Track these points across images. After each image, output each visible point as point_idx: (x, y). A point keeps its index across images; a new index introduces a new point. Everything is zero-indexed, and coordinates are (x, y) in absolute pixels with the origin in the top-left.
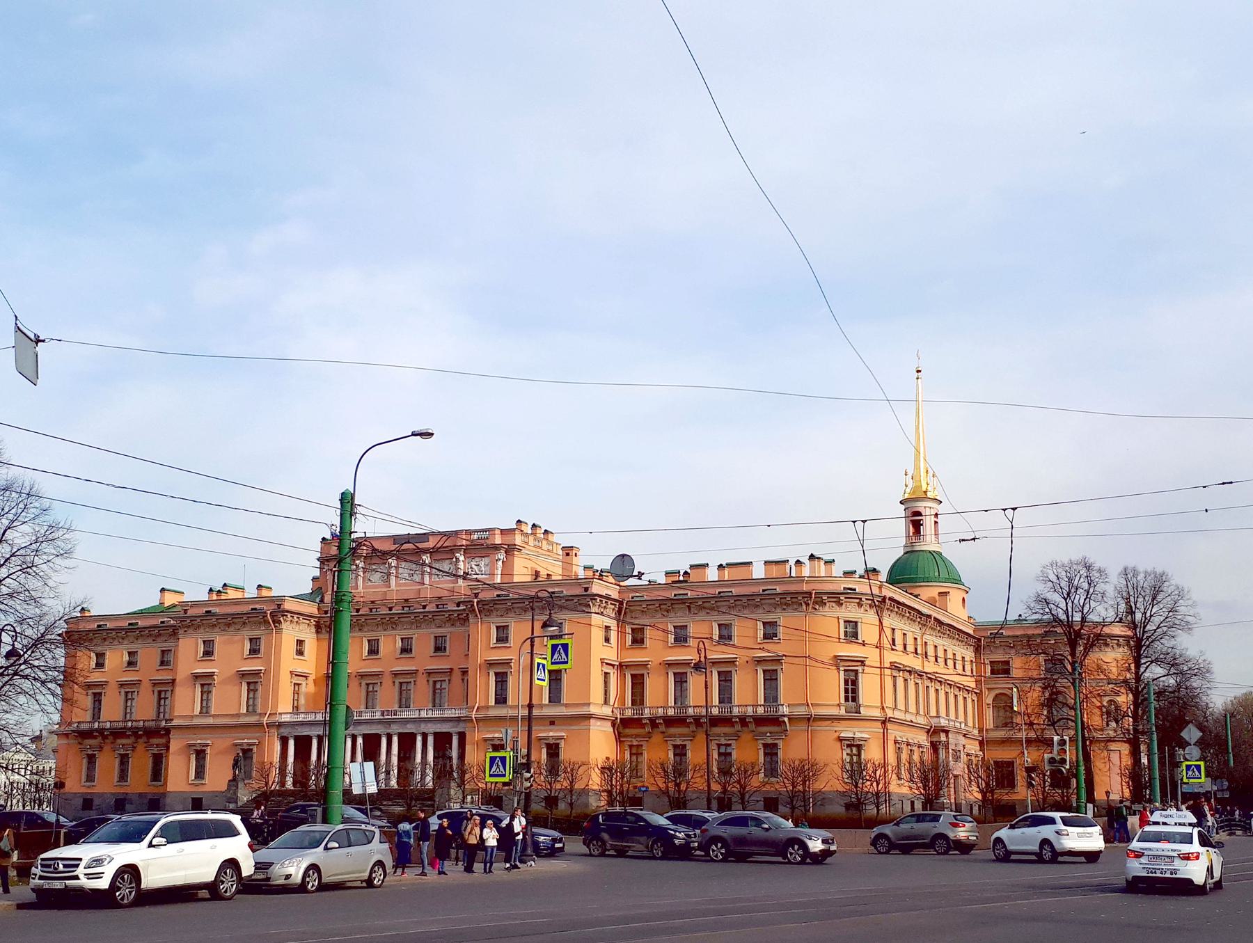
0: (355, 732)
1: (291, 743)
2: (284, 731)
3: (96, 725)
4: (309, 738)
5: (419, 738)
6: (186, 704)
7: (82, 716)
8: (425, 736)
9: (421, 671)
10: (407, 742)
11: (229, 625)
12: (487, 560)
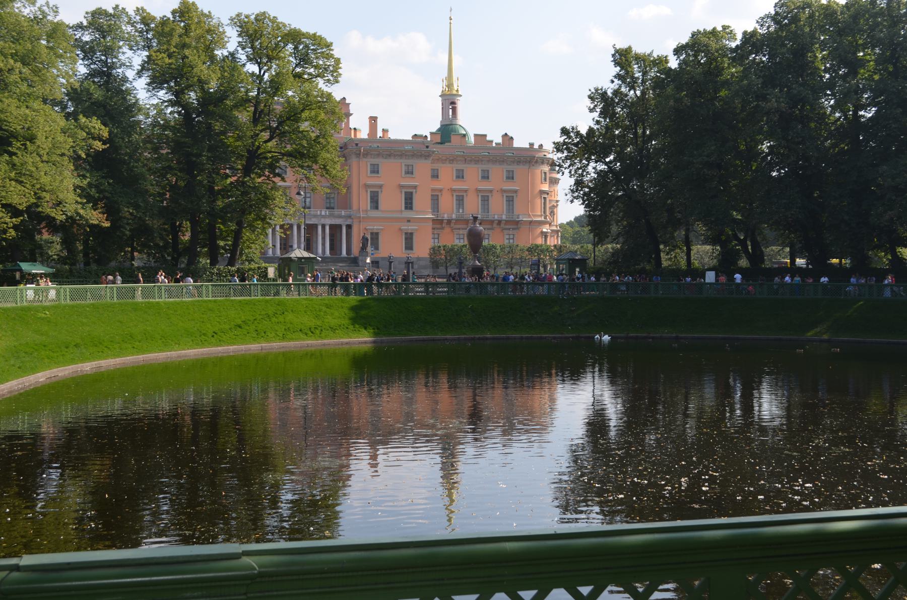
5: (320, 228)
8: (323, 226)
10: (311, 229)
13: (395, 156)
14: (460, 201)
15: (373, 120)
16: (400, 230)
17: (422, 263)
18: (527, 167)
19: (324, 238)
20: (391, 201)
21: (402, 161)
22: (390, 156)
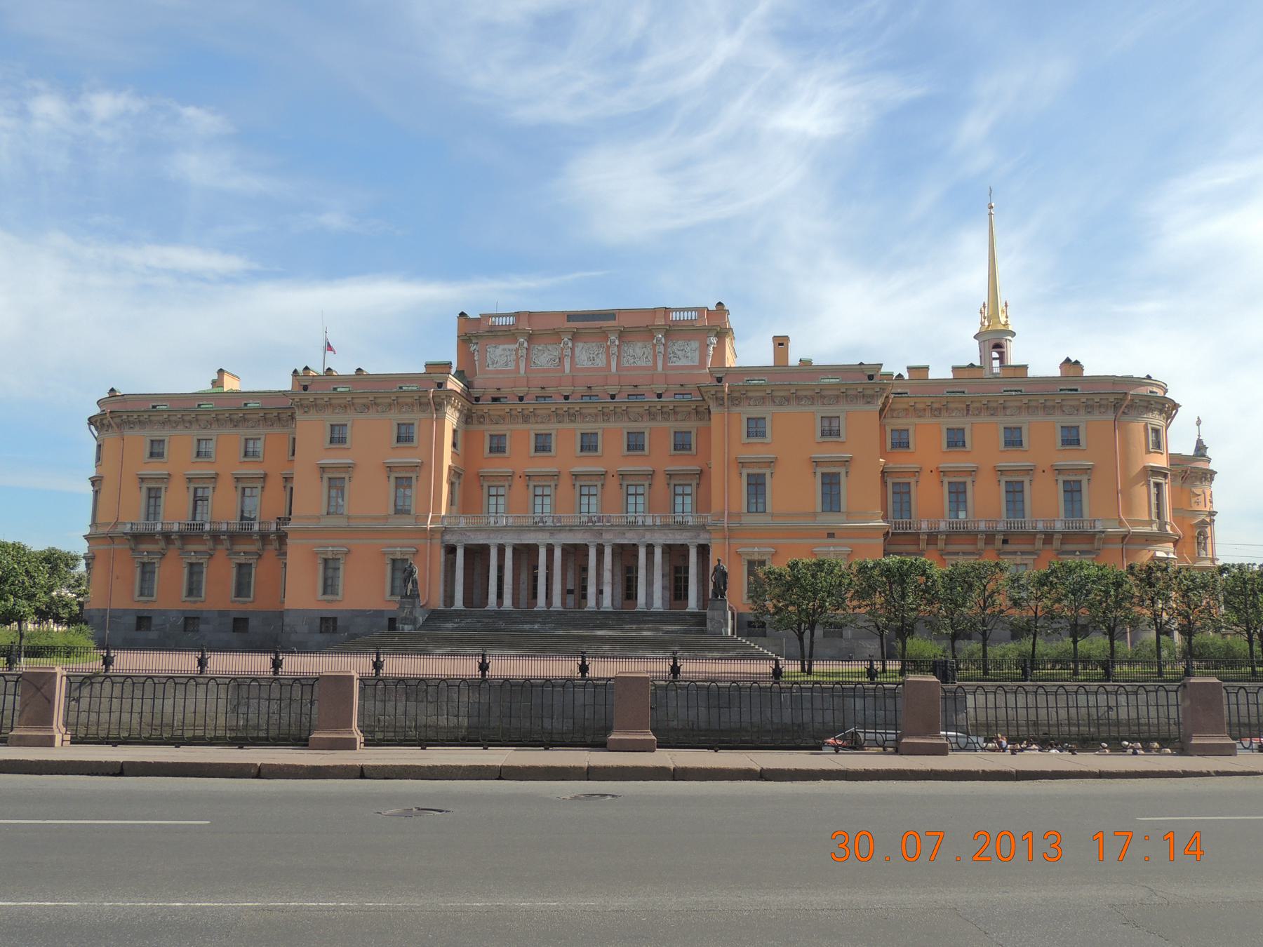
0: (550, 541)
1: (460, 553)
2: (451, 539)
3: (159, 527)
4: (485, 549)
6: (310, 499)
7: (133, 516)
8: (650, 548)
11: (367, 407)
12: (695, 345)
13: (799, 399)
14: (958, 494)
15: (781, 343)
18: (1110, 416)
20: (794, 492)
21: (813, 408)
22: (788, 399)
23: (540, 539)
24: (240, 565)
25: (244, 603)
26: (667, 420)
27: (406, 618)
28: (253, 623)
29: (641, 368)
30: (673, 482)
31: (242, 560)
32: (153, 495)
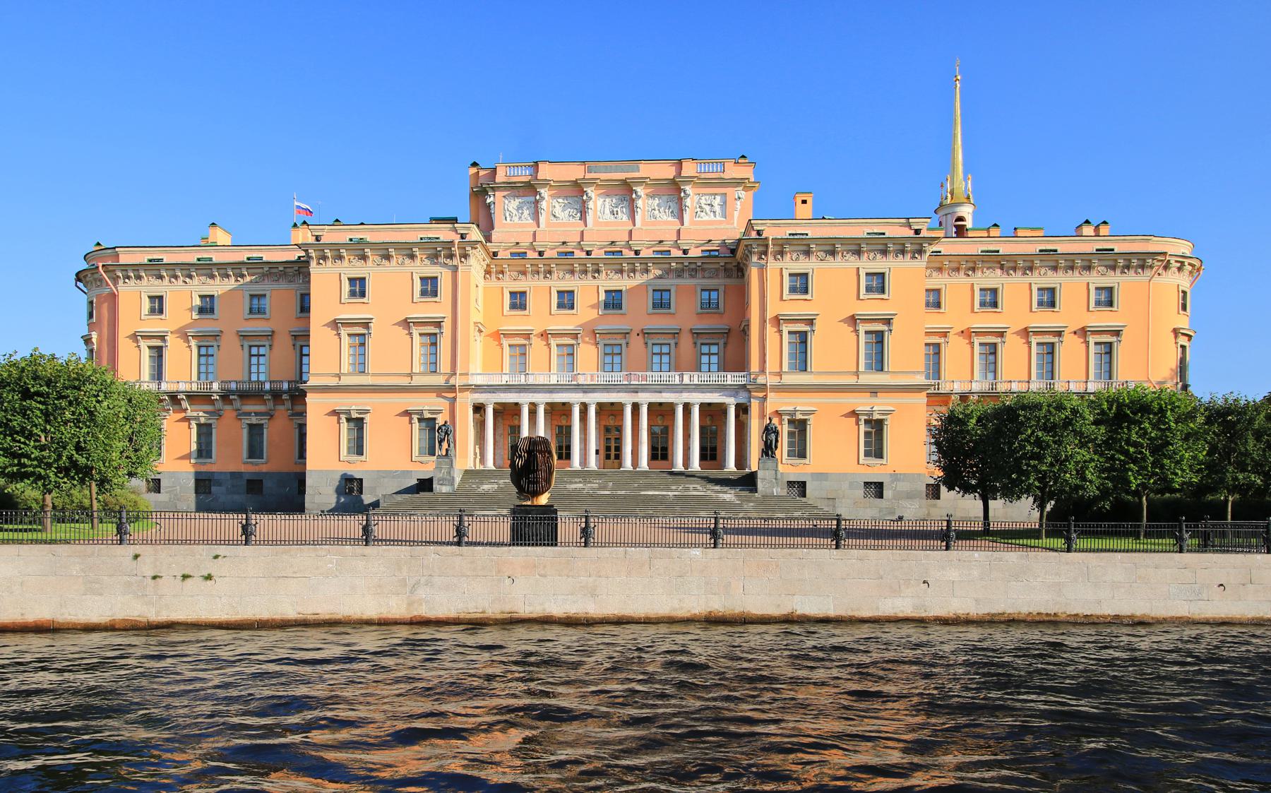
0: (584, 400)
2: (480, 398)
8: (687, 408)
9: (637, 329)
16: (854, 414)
17: (903, 486)
19: (687, 436)
23: (575, 398)
24: (251, 426)
25: (257, 464)
26: (692, 276)
27: (443, 479)
28: (267, 484)
29: (666, 223)
30: (699, 342)
31: (254, 420)
32: (158, 353)
